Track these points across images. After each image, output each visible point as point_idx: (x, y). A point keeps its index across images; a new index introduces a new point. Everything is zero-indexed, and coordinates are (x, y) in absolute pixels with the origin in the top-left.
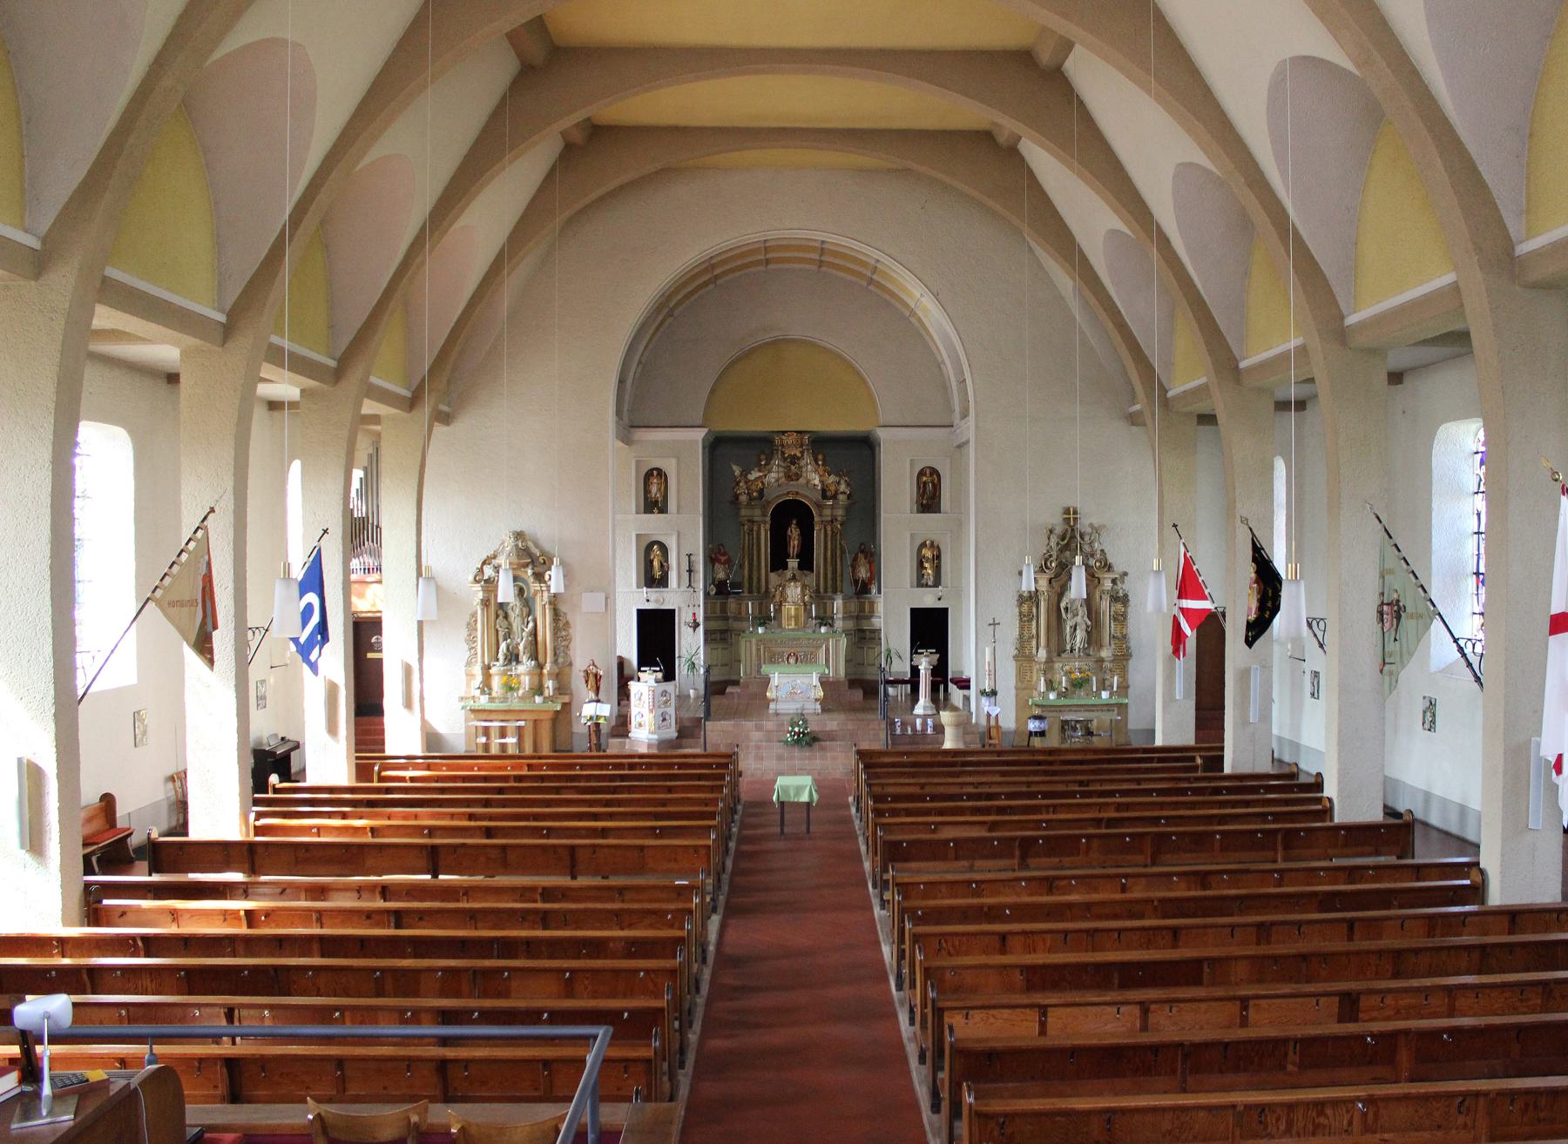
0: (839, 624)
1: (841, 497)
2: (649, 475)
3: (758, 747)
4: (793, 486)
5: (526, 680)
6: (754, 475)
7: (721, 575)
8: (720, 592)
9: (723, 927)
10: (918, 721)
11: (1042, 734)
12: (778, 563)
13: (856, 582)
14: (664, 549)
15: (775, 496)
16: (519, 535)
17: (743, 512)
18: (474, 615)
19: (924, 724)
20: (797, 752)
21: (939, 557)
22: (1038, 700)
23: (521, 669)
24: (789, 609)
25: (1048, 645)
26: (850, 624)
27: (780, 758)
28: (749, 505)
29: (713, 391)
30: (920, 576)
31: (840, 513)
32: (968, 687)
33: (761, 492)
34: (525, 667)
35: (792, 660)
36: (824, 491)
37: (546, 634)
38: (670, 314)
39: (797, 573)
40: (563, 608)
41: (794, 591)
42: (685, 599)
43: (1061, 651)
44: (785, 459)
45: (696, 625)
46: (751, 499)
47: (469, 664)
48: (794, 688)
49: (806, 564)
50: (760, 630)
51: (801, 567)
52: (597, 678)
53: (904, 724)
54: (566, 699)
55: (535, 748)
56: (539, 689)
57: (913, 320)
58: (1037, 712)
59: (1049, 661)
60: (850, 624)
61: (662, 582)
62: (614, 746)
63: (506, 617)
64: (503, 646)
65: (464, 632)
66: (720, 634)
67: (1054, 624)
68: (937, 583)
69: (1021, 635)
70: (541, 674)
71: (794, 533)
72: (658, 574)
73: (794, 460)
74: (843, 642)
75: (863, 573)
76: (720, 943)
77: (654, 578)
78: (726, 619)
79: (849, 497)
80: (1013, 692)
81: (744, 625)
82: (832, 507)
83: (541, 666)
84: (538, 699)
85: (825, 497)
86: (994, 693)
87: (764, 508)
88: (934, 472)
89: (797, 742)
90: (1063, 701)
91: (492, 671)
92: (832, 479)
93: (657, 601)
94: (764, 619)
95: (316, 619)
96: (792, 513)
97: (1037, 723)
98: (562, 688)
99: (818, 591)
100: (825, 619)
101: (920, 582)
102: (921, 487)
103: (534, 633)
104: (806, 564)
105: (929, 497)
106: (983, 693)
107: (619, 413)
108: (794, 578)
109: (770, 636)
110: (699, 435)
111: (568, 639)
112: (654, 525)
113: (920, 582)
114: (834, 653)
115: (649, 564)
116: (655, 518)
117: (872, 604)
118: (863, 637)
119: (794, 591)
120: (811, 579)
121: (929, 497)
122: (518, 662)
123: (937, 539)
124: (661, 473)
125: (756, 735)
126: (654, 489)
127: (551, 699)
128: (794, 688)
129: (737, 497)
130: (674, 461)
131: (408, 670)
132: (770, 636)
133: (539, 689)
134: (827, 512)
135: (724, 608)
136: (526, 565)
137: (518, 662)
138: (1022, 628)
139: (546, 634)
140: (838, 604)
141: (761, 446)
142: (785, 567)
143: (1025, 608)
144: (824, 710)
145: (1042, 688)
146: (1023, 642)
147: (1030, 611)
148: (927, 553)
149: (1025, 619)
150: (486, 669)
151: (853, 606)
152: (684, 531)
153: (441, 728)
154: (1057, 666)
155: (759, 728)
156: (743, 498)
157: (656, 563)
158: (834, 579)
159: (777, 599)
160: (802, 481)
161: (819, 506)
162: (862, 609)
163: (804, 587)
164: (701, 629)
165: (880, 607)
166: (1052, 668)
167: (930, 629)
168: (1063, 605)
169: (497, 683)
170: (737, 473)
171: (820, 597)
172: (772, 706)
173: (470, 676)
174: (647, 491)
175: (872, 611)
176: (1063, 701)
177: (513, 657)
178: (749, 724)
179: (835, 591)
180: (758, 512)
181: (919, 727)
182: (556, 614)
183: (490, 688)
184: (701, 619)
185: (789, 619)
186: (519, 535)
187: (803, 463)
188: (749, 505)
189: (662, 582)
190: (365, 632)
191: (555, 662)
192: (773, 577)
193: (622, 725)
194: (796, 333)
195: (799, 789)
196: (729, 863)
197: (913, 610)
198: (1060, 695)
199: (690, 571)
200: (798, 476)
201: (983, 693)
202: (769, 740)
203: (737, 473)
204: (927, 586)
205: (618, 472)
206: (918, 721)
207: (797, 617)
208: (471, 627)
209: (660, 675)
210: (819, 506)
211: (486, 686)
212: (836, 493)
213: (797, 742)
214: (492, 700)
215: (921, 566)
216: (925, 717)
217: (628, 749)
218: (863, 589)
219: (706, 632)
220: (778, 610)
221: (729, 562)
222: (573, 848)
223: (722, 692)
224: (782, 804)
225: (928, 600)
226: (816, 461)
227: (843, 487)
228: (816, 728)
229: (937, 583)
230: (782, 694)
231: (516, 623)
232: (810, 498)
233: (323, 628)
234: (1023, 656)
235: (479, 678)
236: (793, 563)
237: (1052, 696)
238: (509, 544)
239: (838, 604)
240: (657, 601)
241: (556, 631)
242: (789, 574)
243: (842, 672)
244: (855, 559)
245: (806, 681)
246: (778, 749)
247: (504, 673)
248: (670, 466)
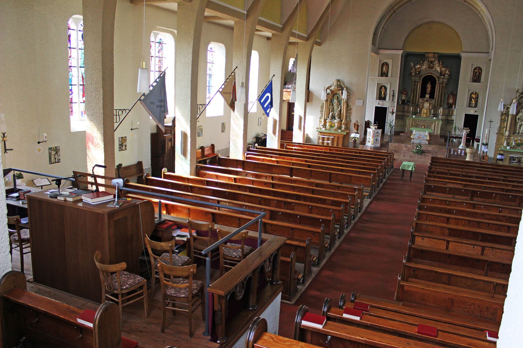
0: (440, 117)
1: (446, 75)
2: (383, 64)
3: (404, 152)
4: (431, 71)
5: (336, 125)
6: (418, 66)
7: (404, 98)
8: (402, 104)
9: (370, 203)
10: (459, 151)
11: (502, 160)
12: (423, 96)
13: (448, 104)
14: (386, 88)
15: (424, 74)
16: (338, 81)
17: (413, 78)
18: (323, 104)
19: (461, 152)
20: (417, 156)
21: (477, 98)
22: (503, 148)
23: (335, 121)
24: (424, 111)
25: (510, 131)
26: (444, 117)
27: (411, 157)
28: (415, 76)
29: (407, 38)
30: (470, 103)
31: (445, 80)
32: (479, 142)
33: (420, 72)
34: (336, 121)
36: (441, 73)
37: (344, 111)
38: (394, 12)
40: (350, 104)
41: (427, 105)
42: (390, 105)
43: (514, 133)
44: (429, 62)
45: (393, 113)
46: (416, 74)
47: (320, 118)
48: (420, 136)
49: (432, 96)
50: (414, 116)
51: (430, 97)
52: (358, 126)
53: (454, 151)
54: (348, 131)
55: (337, 145)
56: (340, 128)
57: (480, 15)
58: (502, 152)
59: (509, 136)
60: (444, 117)
61: (384, 99)
62: (360, 147)
63: (333, 105)
64: (331, 114)
65: (320, 109)
66: (401, 117)
67: (513, 122)
68: (476, 106)
69: (500, 126)
70: (341, 123)
71: (429, 86)
72: (383, 96)
73: (432, 62)
74: (441, 123)
75: (451, 101)
76: (367, 207)
77: (381, 97)
78: (404, 112)
79: (449, 75)
80: (495, 145)
81: (409, 114)
82: (443, 79)
83: (341, 121)
84: (339, 131)
85: (441, 75)
86: (487, 144)
87: (420, 77)
88: (480, 69)
89: (417, 153)
90: (512, 150)
91: (327, 121)
92: (444, 69)
93: (382, 104)
94: (415, 113)
95: (269, 101)
96: (429, 79)
97: (500, 156)
98: (347, 128)
99: (435, 105)
100: (436, 115)
101: (470, 106)
102: (474, 73)
103: (340, 111)
104: (432, 96)
105: (477, 77)
106: (483, 144)
107: (373, 43)
108: (427, 101)
109: (416, 119)
110: (401, 52)
111: (351, 113)
112: (383, 80)
113: (470, 106)
114: (437, 127)
115: (380, 92)
116: (384, 78)
117: (453, 111)
118: (448, 122)
119: (427, 105)
120: (433, 102)
121: (477, 77)
122: (335, 119)
123: (477, 91)
124: (387, 64)
125: (405, 149)
126: (384, 69)
127: (343, 131)
128: (420, 136)
129: (411, 73)
130: (391, 60)
131: (300, 118)
133: (340, 128)
134: (441, 80)
135: (403, 108)
136: (340, 90)
137: (335, 119)
138: (501, 124)
139: (344, 111)
140: (441, 110)
141: (422, 57)
142: (425, 97)
143: (503, 117)
144: (429, 144)
145: (505, 144)
146: (500, 128)
147: (505, 118)
148: (474, 96)
149: (502, 121)
150: (325, 120)
151: (446, 112)
152: (393, 84)
153: (311, 136)
154: (512, 138)
155: (406, 147)
156: (413, 74)
157: (383, 93)
158: (441, 102)
160: (434, 69)
161: (439, 78)
162: (449, 112)
163: (430, 104)
164: (395, 114)
165: (455, 113)
166: (510, 139)
167: (471, 122)
168: (517, 117)
169: (328, 124)
170: (412, 65)
171: (435, 108)
172: (412, 140)
173: (320, 122)
174: (382, 70)
175: (452, 114)
176: (512, 150)
177: (333, 117)
178: (403, 145)
179: (440, 106)
180: (418, 79)
181: (459, 153)
182: (348, 105)
183: (326, 126)
184: (395, 111)
185: (424, 114)
186: (338, 81)
187: (435, 63)
188: (415, 76)
189: (384, 99)
190: (291, 106)
191: (346, 120)
192: (421, 100)
193: (364, 142)
194: (436, 19)
195: (409, 166)
196: (381, 185)
197: (466, 115)
198: (511, 148)
199: (393, 96)
200: (432, 68)
201: (483, 144)
202: (409, 151)
203: (412, 65)
204: (472, 107)
205: (373, 62)
206: (459, 151)
207: (426, 113)
208: (322, 107)
209: (376, 127)
210: (439, 78)
211: (325, 125)
212: (445, 74)
213: (417, 153)
214: (326, 129)
215: (471, 100)
216: (462, 150)
217: (365, 148)
218: (450, 106)
219: (396, 115)
220: (421, 111)
221: (407, 94)
222: (330, 173)
223: (399, 135)
224: (403, 170)
225: (472, 112)
226: (439, 63)
227: (447, 72)
228: (424, 149)
229: (476, 106)
230: (416, 137)
231: (335, 107)
233: (271, 103)
234: (500, 133)
235: (323, 123)
236: (427, 96)
237: (508, 148)
238: (335, 83)
239: (441, 110)
240: (382, 104)
241: (347, 111)
242: (425, 99)
243: (439, 132)
244: (449, 96)
245: (424, 134)
246: (411, 154)
247: (330, 122)
248: (390, 62)
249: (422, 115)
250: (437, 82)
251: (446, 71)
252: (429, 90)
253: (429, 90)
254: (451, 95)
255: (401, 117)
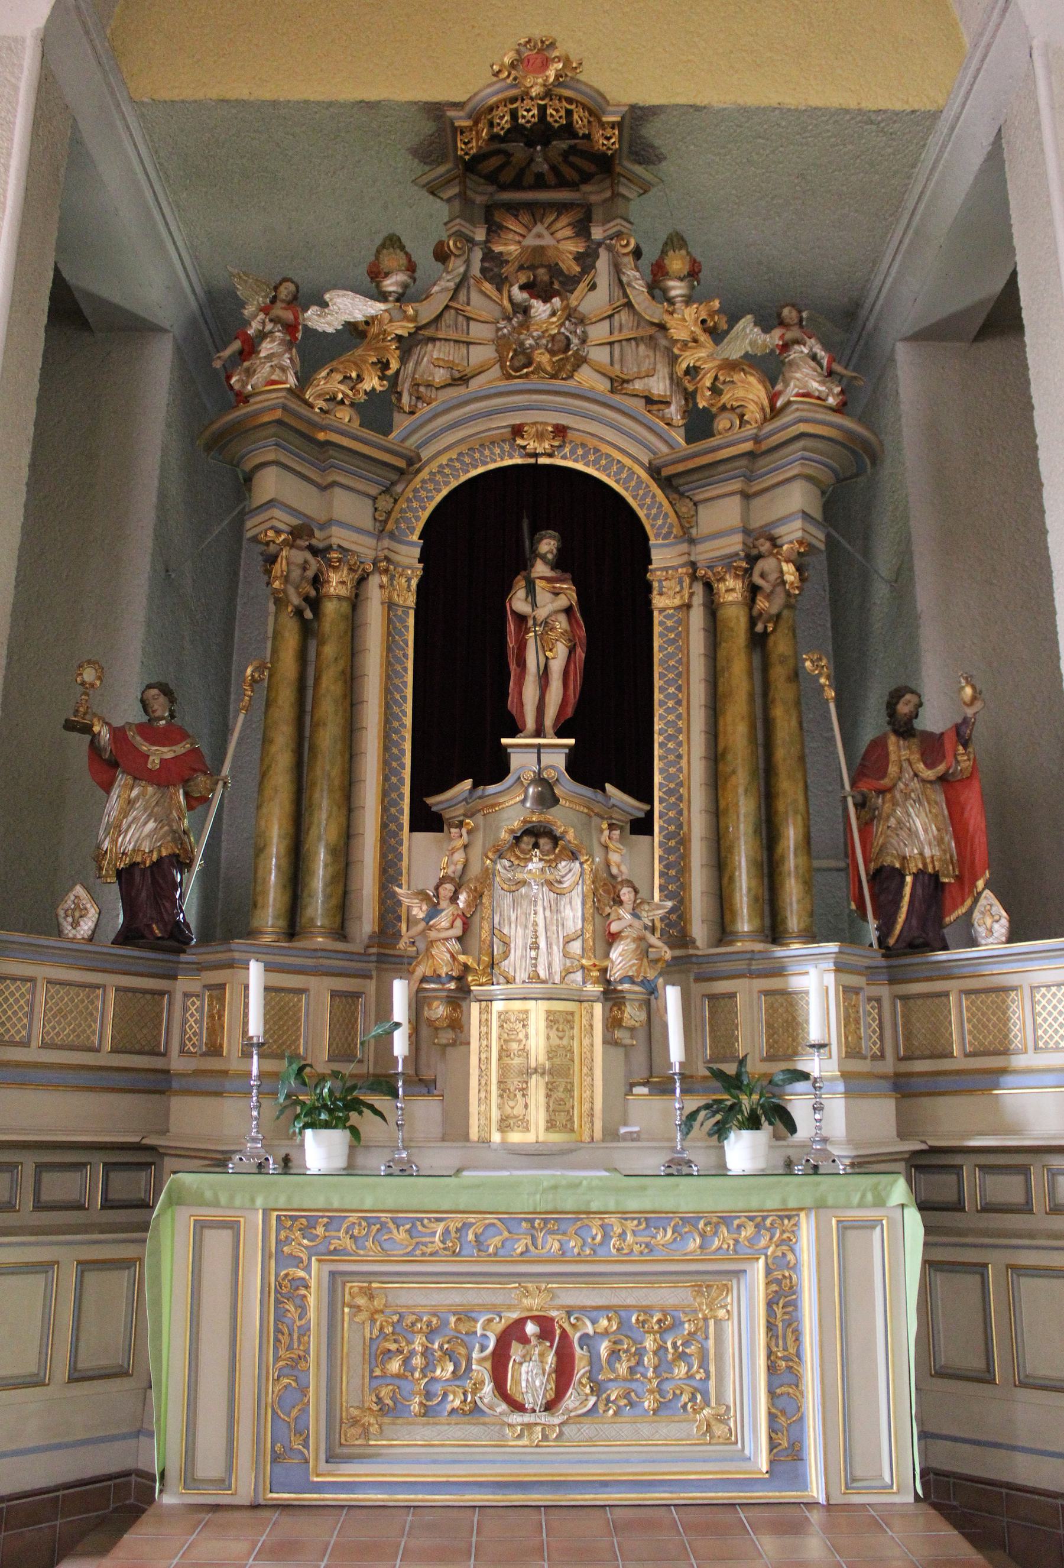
0: (826, 1115)
13: (886, 879)
15: (456, 450)
24: (515, 1025)
35: (530, 1375)
39: (567, 787)
41: (543, 920)
50: (320, 1150)
71: (544, 604)
85: (699, 425)
99: (675, 929)
100: (744, 1095)
108: (536, 834)
109: (379, 1193)
132: (379, 1193)
134: (721, 517)
142: (495, 768)
159: (442, 958)
160: (586, 378)
163: (606, 891)
179: (774, 931)
188: (309, 445)
192: (426, 857)
200: (568, 357)
207: (559, 1074)
220: (442, 1032)
221: (187, 775)
232: (615, 454)
236: (537, 754)
242: (512, 805)
244: (870, 766)
249: (483, 1108)
250: (663, 557)
251: (771, 368)
252: (546, 663)
253: (546, 663)
254: (898, 750)
255: (90, 1184)
